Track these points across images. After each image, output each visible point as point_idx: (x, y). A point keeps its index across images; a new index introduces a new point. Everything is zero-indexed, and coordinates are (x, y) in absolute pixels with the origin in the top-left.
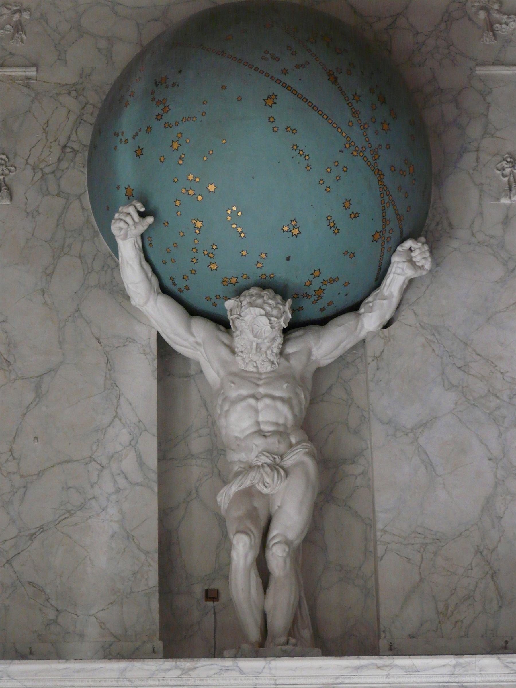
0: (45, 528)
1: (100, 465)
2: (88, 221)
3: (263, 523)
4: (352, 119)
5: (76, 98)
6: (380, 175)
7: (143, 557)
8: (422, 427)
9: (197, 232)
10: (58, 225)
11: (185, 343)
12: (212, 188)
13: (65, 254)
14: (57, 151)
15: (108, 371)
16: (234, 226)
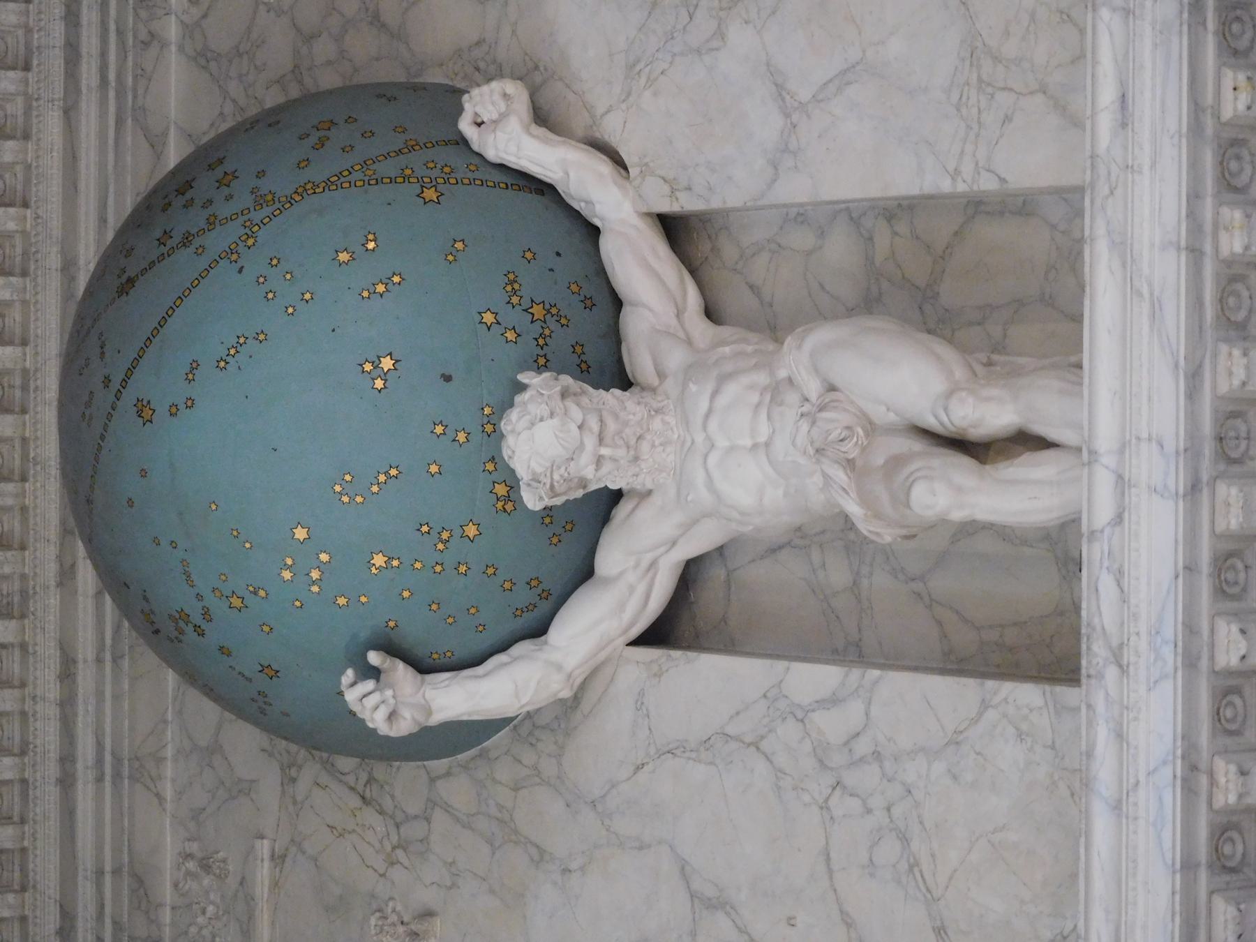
0: (938, 923)
1: (834, 788)
2: (465, 767)
3: (917, 445)
5: (300, 767)
6: (302, 191)
7: (991, 715)
8: (784, 93)
9: (395, 563)
11: (641, 589)
12: (301, 534)
13: (512, 819)
15: (687, 754)
16: (375, 489)
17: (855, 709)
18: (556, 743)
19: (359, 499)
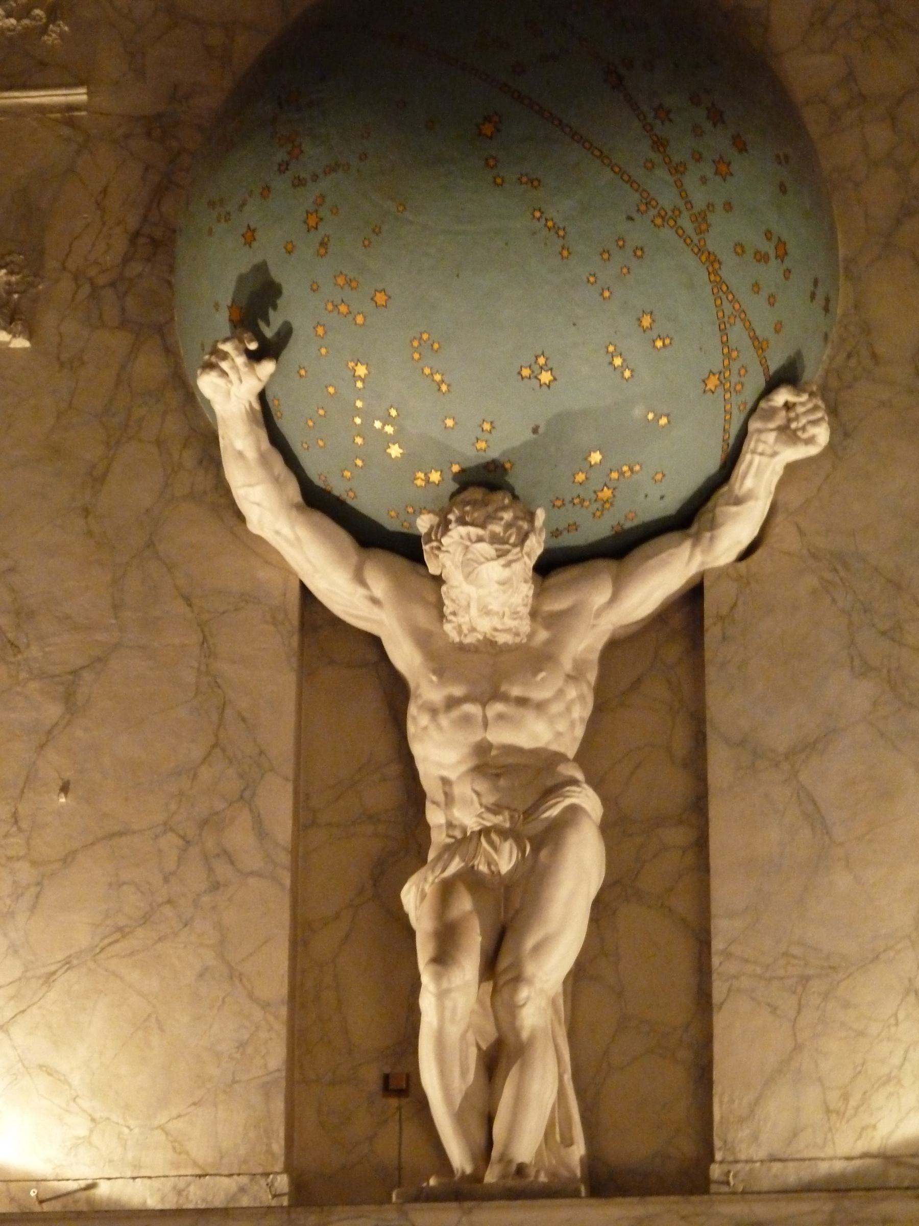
4: (652, 155)
7: (258, 1014)
10: (118, 382)
14: (120, 245)
16: (427, 371)
17: (252, 860)
18: (205, 492)
19: (416, 356)
